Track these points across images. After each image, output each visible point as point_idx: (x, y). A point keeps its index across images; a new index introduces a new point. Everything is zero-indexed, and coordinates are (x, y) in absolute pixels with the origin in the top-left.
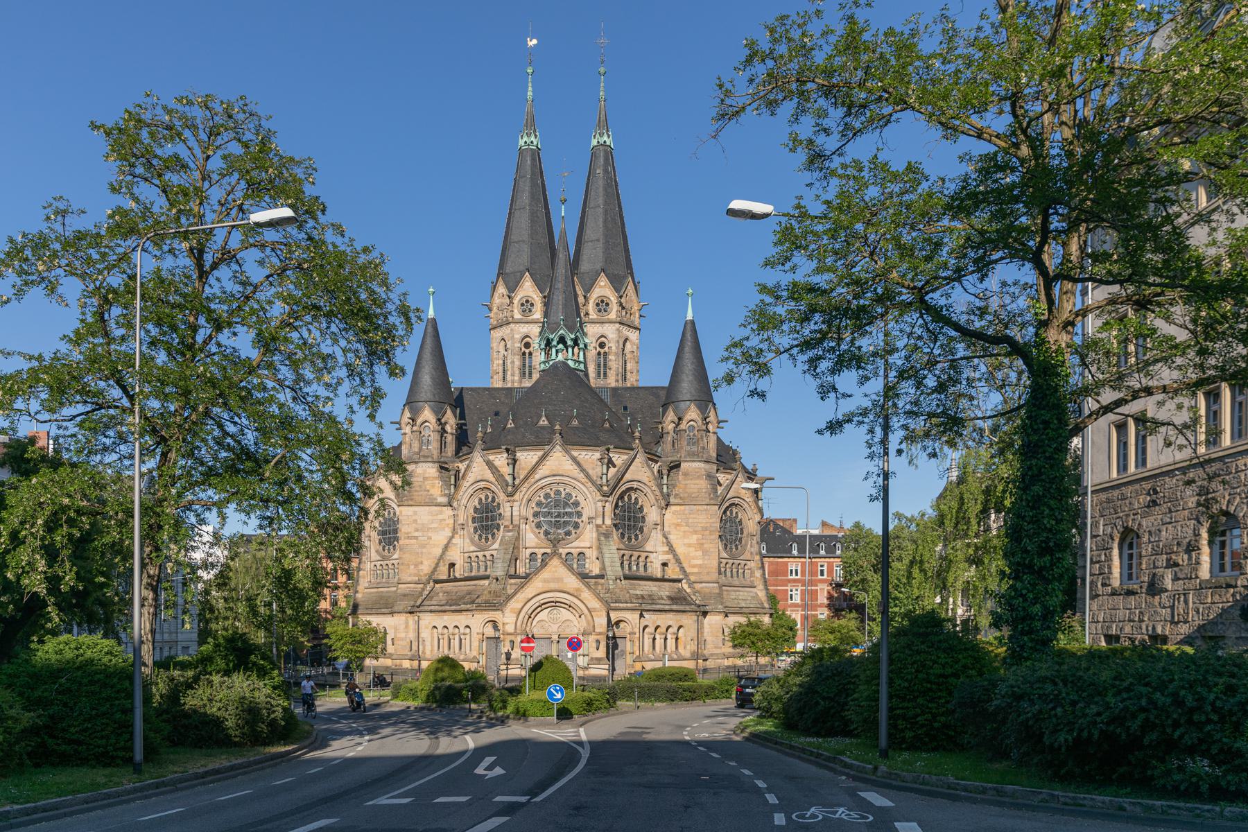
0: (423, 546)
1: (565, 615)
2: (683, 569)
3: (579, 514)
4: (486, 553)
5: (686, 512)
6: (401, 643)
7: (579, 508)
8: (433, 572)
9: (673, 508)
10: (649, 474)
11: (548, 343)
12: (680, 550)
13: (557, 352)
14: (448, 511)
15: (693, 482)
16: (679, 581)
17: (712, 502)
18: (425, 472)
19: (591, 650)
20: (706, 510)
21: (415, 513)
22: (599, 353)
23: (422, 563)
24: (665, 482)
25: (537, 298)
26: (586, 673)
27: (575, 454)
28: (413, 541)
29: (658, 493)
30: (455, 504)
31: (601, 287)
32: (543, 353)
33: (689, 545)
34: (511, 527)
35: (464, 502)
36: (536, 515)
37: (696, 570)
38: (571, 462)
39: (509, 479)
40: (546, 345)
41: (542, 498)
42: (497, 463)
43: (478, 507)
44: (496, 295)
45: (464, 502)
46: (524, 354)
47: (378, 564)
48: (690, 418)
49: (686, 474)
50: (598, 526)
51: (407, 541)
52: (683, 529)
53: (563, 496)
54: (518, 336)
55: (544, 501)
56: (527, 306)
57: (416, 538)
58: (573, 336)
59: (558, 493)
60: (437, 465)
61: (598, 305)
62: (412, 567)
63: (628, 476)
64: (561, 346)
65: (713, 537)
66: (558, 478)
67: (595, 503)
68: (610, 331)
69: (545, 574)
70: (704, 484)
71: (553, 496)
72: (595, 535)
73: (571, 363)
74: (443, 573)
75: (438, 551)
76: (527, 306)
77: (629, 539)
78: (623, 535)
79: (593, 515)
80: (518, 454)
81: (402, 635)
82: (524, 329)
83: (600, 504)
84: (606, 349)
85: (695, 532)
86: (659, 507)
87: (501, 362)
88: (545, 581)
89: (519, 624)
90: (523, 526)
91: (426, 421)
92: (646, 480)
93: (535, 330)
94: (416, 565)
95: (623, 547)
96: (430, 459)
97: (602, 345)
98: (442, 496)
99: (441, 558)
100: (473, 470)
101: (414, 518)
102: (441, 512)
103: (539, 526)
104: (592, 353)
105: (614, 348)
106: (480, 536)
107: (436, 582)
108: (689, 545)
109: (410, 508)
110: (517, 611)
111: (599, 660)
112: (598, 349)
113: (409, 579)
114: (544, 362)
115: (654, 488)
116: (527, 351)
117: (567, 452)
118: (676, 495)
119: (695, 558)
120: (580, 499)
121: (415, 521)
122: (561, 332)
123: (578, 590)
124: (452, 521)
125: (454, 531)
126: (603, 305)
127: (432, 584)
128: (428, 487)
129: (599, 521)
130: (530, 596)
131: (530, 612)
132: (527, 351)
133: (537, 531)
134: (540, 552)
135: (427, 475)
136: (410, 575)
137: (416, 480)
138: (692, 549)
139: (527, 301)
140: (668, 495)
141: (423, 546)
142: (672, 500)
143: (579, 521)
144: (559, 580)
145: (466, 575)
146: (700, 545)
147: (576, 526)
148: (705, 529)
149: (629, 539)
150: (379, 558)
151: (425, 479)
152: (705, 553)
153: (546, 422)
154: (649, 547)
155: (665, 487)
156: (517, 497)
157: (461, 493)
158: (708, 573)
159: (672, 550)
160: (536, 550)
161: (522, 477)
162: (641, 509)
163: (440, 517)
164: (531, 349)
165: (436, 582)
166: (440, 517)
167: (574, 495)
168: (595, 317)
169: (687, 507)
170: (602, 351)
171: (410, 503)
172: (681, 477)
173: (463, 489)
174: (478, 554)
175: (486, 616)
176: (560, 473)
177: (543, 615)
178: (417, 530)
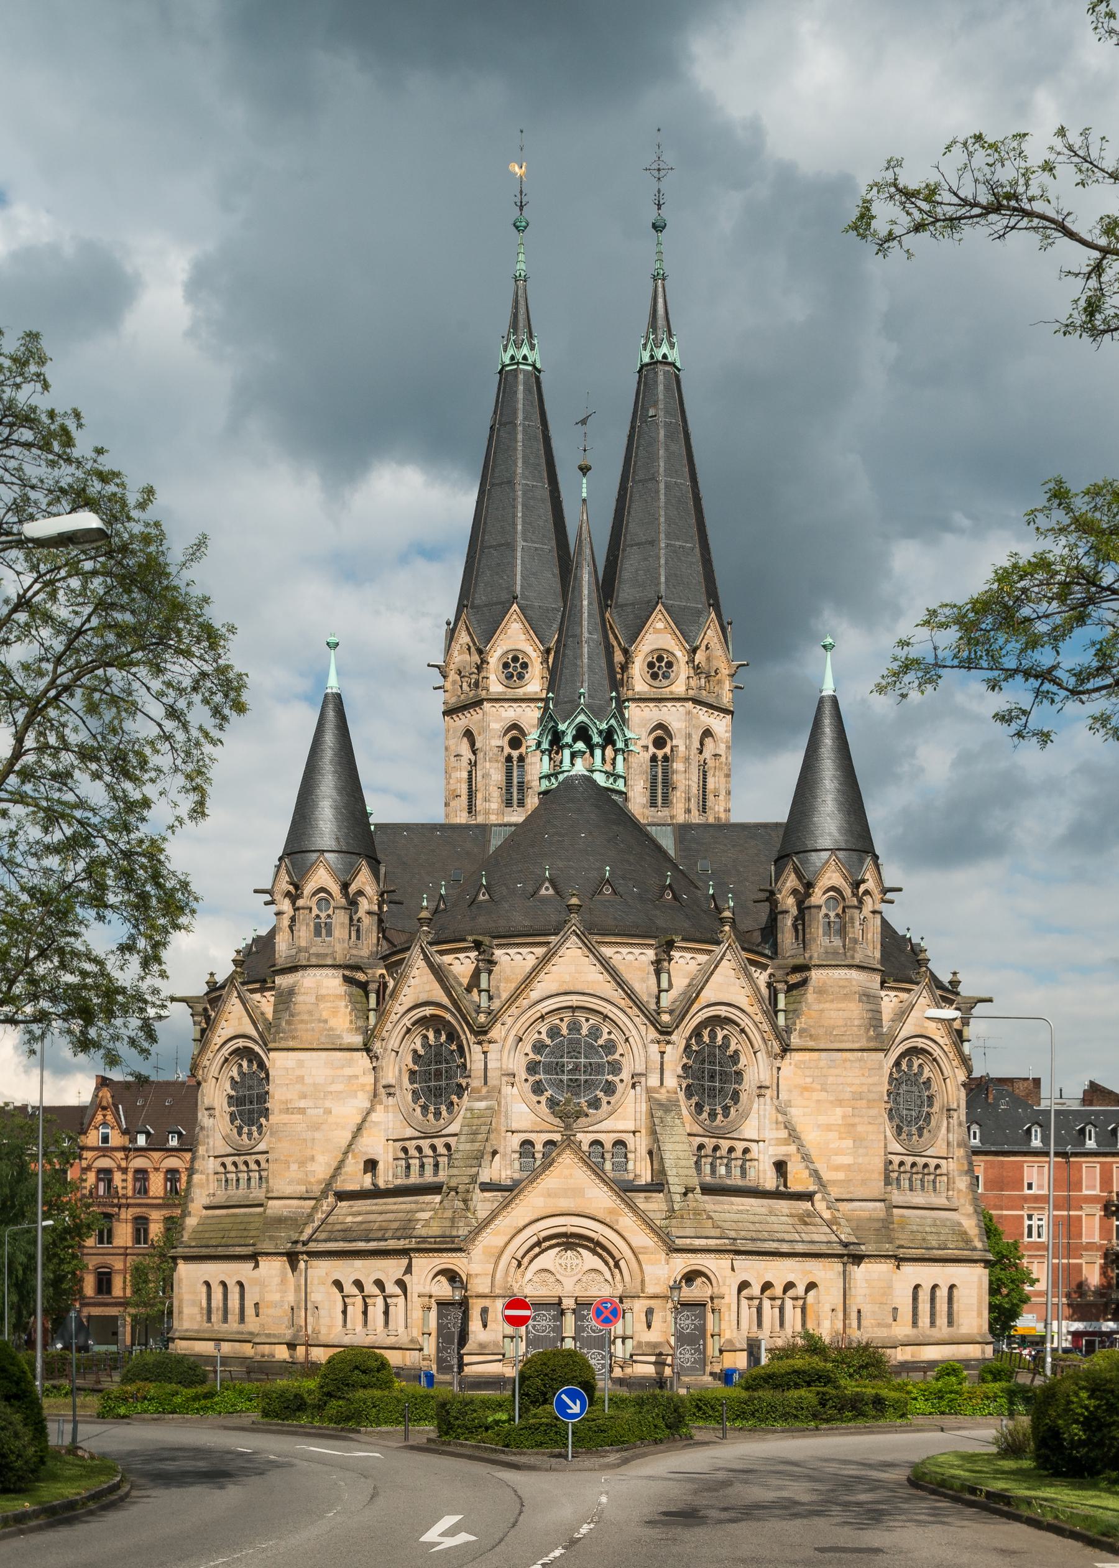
0: (316, 1127)
1: (590, 1260)
2: (816, 1174)
3: (616, 1068)
4: (436, 1141)
5: (822, 1064)
6: (271, 1311)
7: (617, 1056)
8: (334, 1176)
9: (797, 1056)
10: (748, 991)
11: (556, 738)
12: (811, 1136)
13: (573, 755)
15: (834, 1006)
16: (808, 1196)
17: (872, 1045)
18: (319, 986)
20: (860, 1060)
22: (654, 759)
23: (312, 1159)
24: (781, 1005)
25: (532, 652)
26: (628, 1371)
27: (607, 951)
28: (297, 1117)
29: (765, 1027)
30: (377, 1047)
31: (657, 631)
32: (546, 758)
33: (828, 1128)
34: (484, 1090)
35: (394, 1042)
36: (532, 1068)
37: (841, 1176)
40: (552, 744)
41: (544, 1036)
43: (421, 1052)
44: (456, 648)
46: (509, 759)
47: (228, 1161)
48: (829, 883)
49: (821, 991)
50: (648, 1090)
51: (285, 1118)
52: (816, 1096)
53: (584, 1031)
54: (497, 726)
55: (548, 1041)
56: (515, 667)
57: (302, 1111)
58: (604, 726)
60: (339, 973)
61: (651, 665)
62: (294, 1167)
63: (707, 995)
64: (580, 745)
65: (873, 1112)
67: (645, 1046)
68: (674, 716)
69: (550, 1181)
70: (855, 1011)
71: (565, 1032)
72: (644, 1107)
73: (600, 779)
74: (355, 1179)
76: (515, 667)
77: (713, 1115)
78: (699, 1108)
79: (640, 1069)
80: (498, 953)
81: (276, 1297)
82: (510, 713)
83: (654, 1049)
84: (667, 750)
85: (840, 1102)
86: (769, 1054)
87: (465, 775)
88: (550, 1194)
89: (499, 1275)
90: (507, 1090)
91: (322, 890)
92: (743, 1002)
93: (530, 716)
94: (302, 1164)
95: (700, 1131)
96: (329, 962)
97: (659, 743)
98: (350, 1030)
100: (412, 982)
101: (299, 1072)
102: (350, 1063)
103: (538, 1089)
104: (641, 759)
105: (682, 748)
106: (425, 1108)
107: (341, 1196)
108: (828, 1128)
109: (291, 1054)
110: (496, 1251)
112: (652, 750)
113: (288, 1190)
114: (548, 777)
115: (759, 1018)
116: (515, 754)
117: (591, 950)
118: (802, 1031)
119: (838, 1152)
121: (300, 1079)
122: (582, 718)
123: (611, 1212)
124: (370, 1079)
126: (660, 666)
127: (331, 1199)
129: (653, 1081)
130: (521, 1224)
131: (519, 1255)
132: (515, 754)
133: (536, 1098)
134: (539, 1140)
135: (323, 992)
136: (289, 1183)
137: (303, 1001)
138: (833, 1135)
139: (515, 659)
140: (788, 1030)
141: (316, 1127)
142: (795, 1040)
143: (617, 1079)
144: (578, 1192)
145: (399, 1182)
146: (849, 1128)
147: (610, 1089)
148: (858, 1096)
149: (713, 1115)
150: (230, 1150)
151: (320, 998)
152: (858, 1141)
153: (551, 892)
154: (749, 1130)
155: (781, 1017)
156: (496, 1032)
157: (389, 1026)
158: (864, 1182)
159: (794, 1136)
160: (532, 1137)
161: (505, 995)
162: (735, 1057)
163: (348, 1071)
164: (523, 750)
165: (341, 1196)
166: (348, 1071)
168: (646, 688)
169: (824, 1054)
170: (660, 754)
171: (291, 1044)
172: (810, 996)
173: (394, 1018)
174: (421, 1142)
175: (437, 1261)
176: (579, 988)
178: (304, 1096)
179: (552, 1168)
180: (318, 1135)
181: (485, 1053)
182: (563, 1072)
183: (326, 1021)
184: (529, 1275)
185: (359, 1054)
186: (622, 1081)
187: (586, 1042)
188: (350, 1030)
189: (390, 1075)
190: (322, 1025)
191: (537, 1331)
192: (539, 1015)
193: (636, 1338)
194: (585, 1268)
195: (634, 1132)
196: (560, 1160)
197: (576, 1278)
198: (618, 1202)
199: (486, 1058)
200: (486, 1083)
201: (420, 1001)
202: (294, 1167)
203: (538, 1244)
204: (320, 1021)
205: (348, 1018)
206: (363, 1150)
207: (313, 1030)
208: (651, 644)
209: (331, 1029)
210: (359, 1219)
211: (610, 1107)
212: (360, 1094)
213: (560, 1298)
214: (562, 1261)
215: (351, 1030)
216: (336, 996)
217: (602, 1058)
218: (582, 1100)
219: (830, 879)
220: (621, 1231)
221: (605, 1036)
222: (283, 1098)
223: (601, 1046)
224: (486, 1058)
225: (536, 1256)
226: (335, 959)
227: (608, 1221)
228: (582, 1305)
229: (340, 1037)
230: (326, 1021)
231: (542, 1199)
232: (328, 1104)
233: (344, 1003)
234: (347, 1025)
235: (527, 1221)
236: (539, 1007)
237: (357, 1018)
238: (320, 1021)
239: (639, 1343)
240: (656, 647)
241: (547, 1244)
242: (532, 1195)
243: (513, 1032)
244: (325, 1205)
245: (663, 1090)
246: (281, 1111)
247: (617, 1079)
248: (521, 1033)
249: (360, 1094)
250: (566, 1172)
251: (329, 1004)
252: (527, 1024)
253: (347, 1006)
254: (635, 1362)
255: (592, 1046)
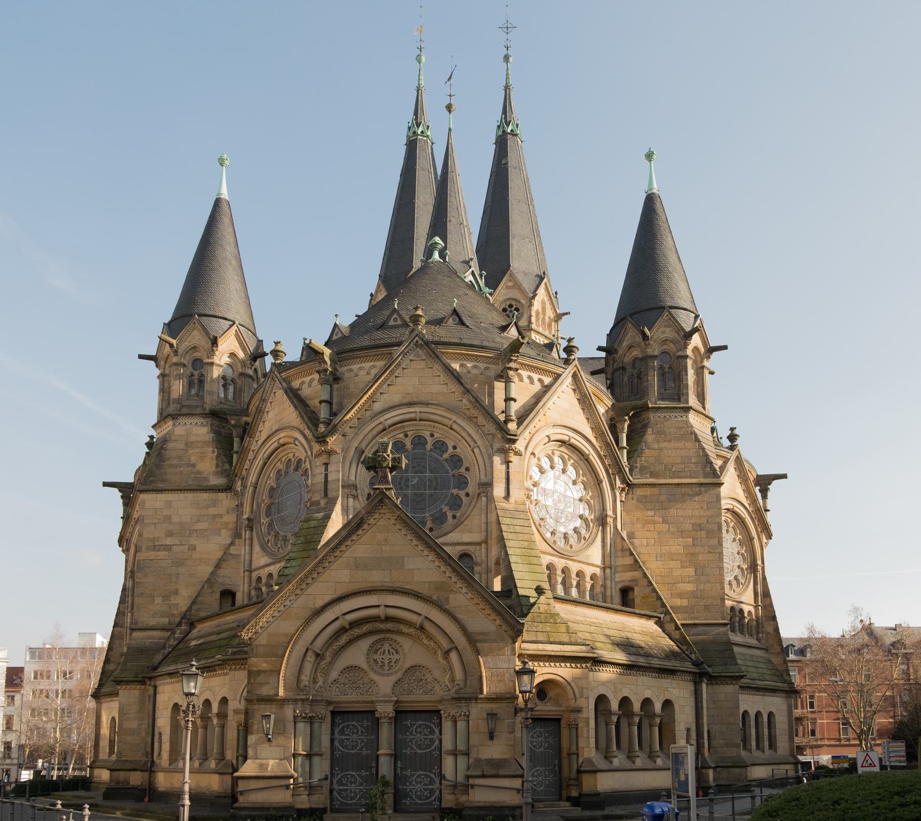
14: (226, 501)
19: (475, 739)
21: (169, 504)
23: (176, 592)
28: (162, 554)
30: (238, 486)
34: (323, 502)
35: (252, 479)
38: (443, 378)
39: (323, 413)
42: (306, 392)
45: (252, 479)
51: (152, 554)
53: (429, 446)
57: (168, 548)
59: (419, 441)
62: (158, 600)
66: (418, 409)
75: (205, 571)
88: (357, 565)
94: (166, 597)
96: (199, 411)
98: (216, 474)
99: (210, 581)
101: (166, 513)
102: (215, 503)
111: (495, 769)
120: (463, 451)
121: (168, 518)
123: (440, 587)
125: (237, 535)
128: (193, 459)
130: (320, 603)
135: (193, 439)
141: (180, 563)
143: (462, 493)
147: (456, 504)
163: (213, 511)
166: (213, 511)
167: (450, 444)
173: (251, 455)
176: (423, 399)
177: (357, 655)
178: (170, 534)
179: (360, 532)
180: (182, 570)
181: (326, 464)
182: (407, 486)
183: (194, 465)
184: (334, 675)
185: (222, 495)
186: (467, 495)
187: (430, 457)
188: (216, 474)
189: (248, 509)
190: (190, 469)
191: (346, 747)
192: (381, 427)
193: (473, 755)
194: (407, 666)
195: (479, 544)
196: (372, 521)
197: (394, 678)
198: (448, 574)
199: (326, 470)
200: (326, 495)
201: (273, 430)
202: (158, 600)
203: (343, 630)
204: (188, 465)
205: (215, 462)
206: (220, 580)
207: (181, 473)
208: (504, 296)
209: (199, 472)
210: (201, 641)
211: (456, 521)
212: (224, 532)
213: (372, 702)
214: (378, 657)
215: (218, 473)
216: (204, 442)
217: (447, 472)
218: (427, 515)
219: (663, 333)
220: (452, 610)
221: (451, 450)
222: (151, 536)
223: (446, 460)
224: (326, 470)
225: (343, 647)
226: (205, 409)
227: (435, 597)
228: (401, 714)
229: (206, 479)
230: (194, 465)
231: (347, 572)
232: (193, 541)
233: (211, 449)
234: (213, 468)
235: (327, 599)
236: (382, 419)
237: (223, 463)
238: (188, 465)
239: (478, 760)
240: (507, 297)
241: (357, 631)
242: (334, 566)
243: (355, 444)
244: (178, 632)
245: (512, 500)
246: (148, 548)
247: (462, 493)
248: (363, 445)
249: (224, 532)
250: (380, 537)
251: (197, 450)
252: (370, 436)
253: (213, 452)
254: (473, 786)
255: (438, 460)
